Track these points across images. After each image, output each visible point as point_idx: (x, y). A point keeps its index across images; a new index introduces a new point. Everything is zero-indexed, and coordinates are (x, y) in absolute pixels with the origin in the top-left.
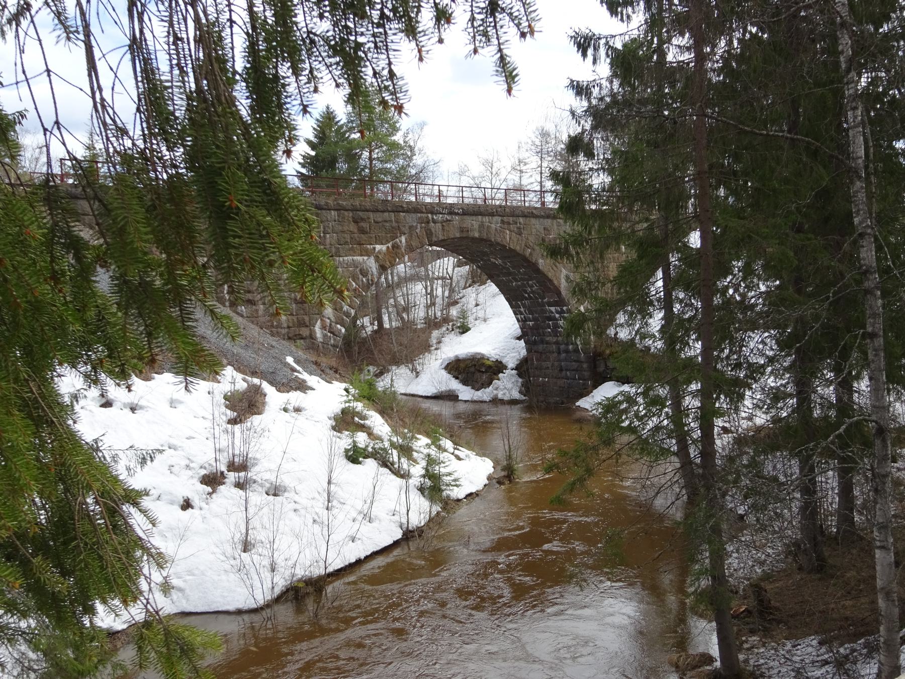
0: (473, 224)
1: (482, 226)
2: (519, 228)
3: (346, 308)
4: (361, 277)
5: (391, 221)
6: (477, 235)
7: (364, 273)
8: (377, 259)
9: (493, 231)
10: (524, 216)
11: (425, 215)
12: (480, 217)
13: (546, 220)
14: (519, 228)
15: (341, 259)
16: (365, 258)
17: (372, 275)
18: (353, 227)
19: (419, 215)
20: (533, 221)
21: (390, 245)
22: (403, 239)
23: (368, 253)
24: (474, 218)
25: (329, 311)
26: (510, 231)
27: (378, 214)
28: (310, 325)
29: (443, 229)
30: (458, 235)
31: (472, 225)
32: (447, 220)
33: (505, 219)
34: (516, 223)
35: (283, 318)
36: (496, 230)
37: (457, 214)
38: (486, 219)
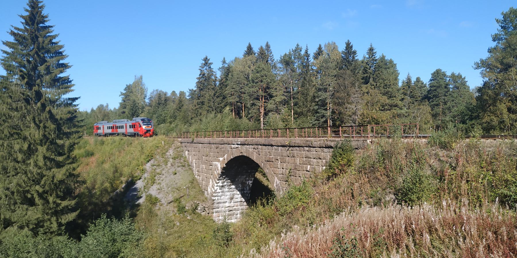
3: (214, 182)
4: (217, 170)
6: (245, 155)
8: (221, 164)
10: (261, 145)
12: (246, 146)
15: (214, 163)
18: (216, 150)
21: (223, 158)
22: (226, 156)
23: (219, 161)
24: (245, 146)
25: (211, 182)
28: (207, 186)
30: (241, 154)
35: (204, 182)
38: (248, 146)
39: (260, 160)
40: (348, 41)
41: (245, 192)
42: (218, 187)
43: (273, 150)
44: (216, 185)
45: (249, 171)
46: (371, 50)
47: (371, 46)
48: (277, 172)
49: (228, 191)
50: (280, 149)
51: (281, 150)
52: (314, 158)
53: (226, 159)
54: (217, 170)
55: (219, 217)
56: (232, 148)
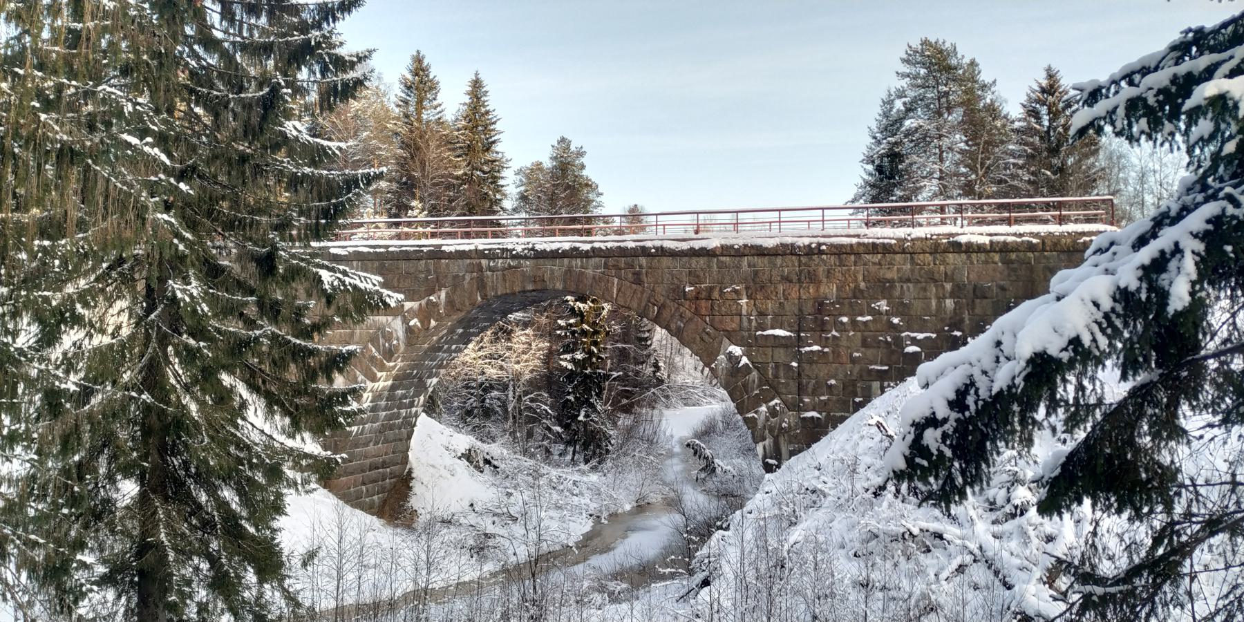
0: (557, 268)
1: (569, 270)
2: (637, 274)
5: (428, 271)
7: (388, 337)
9: (588, 282)
11: (478, 261)
13: (694, 261)
14: (637, 274)
16: (390, 318)
17: (398, 339)
19: (468, 261)
20: (666, 261)
21: (423, 302)
22: (443, 294)
26: (620, 278)
27: (411, 264)
29: (504, 280)
30: (530, 287)
31: (552, 272)
32: (510, 267)
33: (611, 261)
34: (632, 267)
36: (594, 278)
37: (526, 257)
39: (640, 299)
40: (418, 51)
41: (414, 410)
42: (370, 394)
43: (709, 266)
44: (370, 385)
45: (454, 347)
46: (477, 85)
47: (477, 74)
48: (734, 325)
49: (386, 408)
50: (746, 263)
51: (749, 266)
52: (908, 280)
53: (442, 307)
54: (381, 341)
55: (349, 488)
56: (480, 269)
